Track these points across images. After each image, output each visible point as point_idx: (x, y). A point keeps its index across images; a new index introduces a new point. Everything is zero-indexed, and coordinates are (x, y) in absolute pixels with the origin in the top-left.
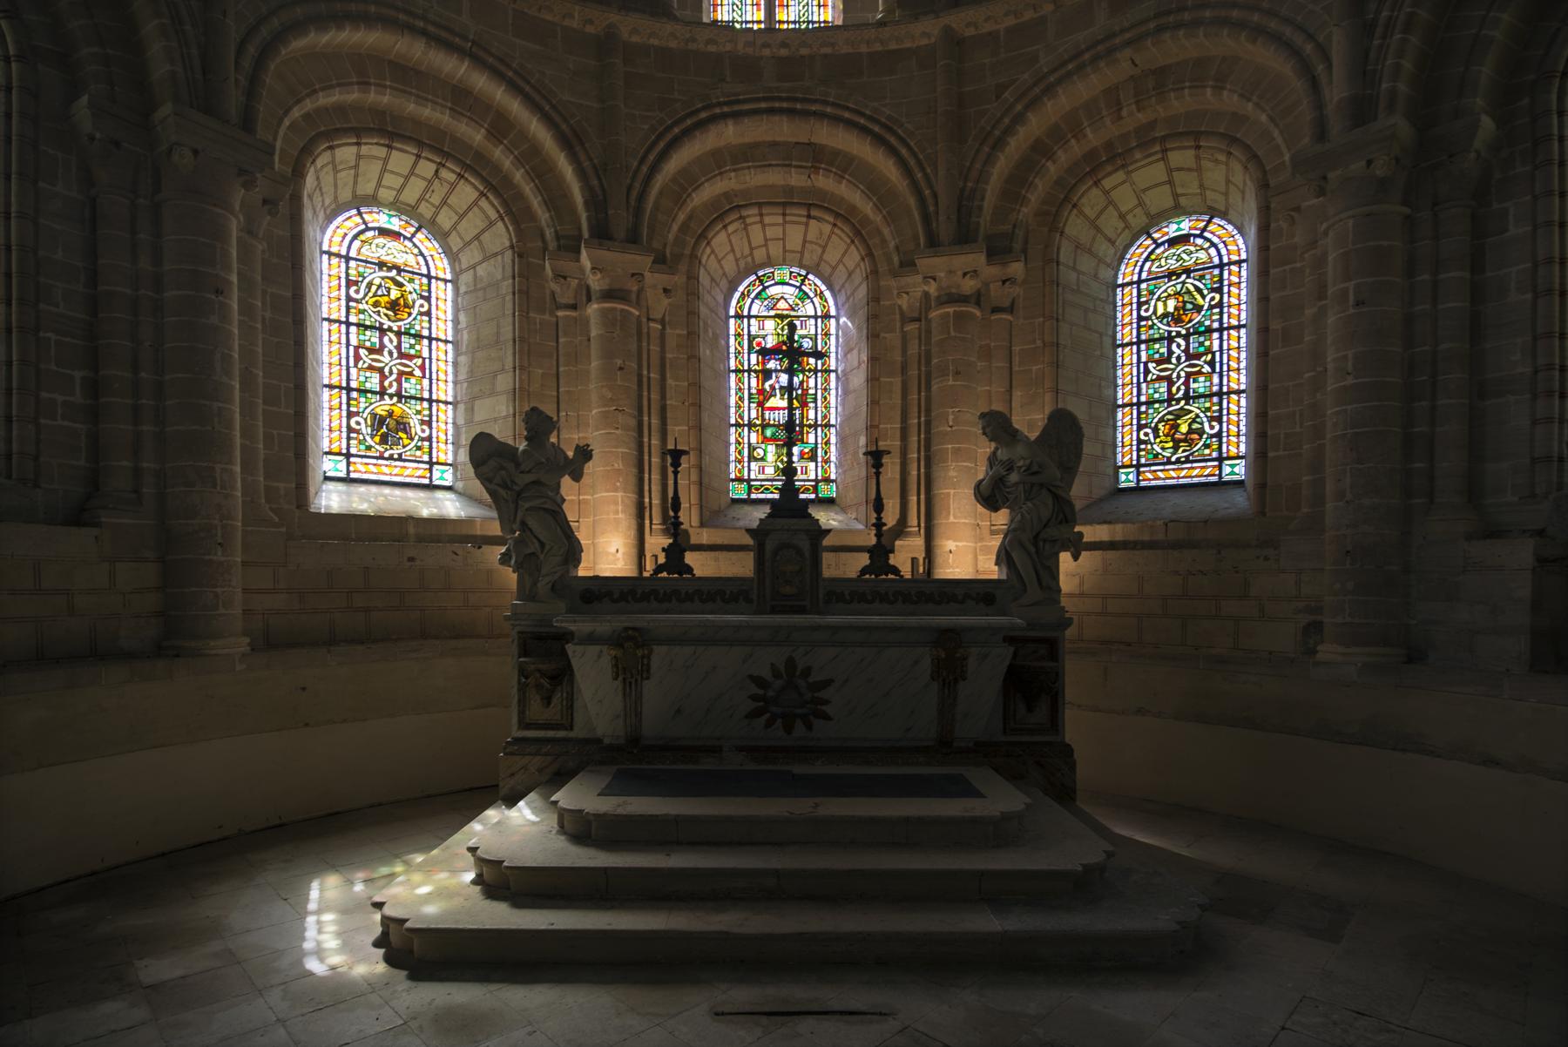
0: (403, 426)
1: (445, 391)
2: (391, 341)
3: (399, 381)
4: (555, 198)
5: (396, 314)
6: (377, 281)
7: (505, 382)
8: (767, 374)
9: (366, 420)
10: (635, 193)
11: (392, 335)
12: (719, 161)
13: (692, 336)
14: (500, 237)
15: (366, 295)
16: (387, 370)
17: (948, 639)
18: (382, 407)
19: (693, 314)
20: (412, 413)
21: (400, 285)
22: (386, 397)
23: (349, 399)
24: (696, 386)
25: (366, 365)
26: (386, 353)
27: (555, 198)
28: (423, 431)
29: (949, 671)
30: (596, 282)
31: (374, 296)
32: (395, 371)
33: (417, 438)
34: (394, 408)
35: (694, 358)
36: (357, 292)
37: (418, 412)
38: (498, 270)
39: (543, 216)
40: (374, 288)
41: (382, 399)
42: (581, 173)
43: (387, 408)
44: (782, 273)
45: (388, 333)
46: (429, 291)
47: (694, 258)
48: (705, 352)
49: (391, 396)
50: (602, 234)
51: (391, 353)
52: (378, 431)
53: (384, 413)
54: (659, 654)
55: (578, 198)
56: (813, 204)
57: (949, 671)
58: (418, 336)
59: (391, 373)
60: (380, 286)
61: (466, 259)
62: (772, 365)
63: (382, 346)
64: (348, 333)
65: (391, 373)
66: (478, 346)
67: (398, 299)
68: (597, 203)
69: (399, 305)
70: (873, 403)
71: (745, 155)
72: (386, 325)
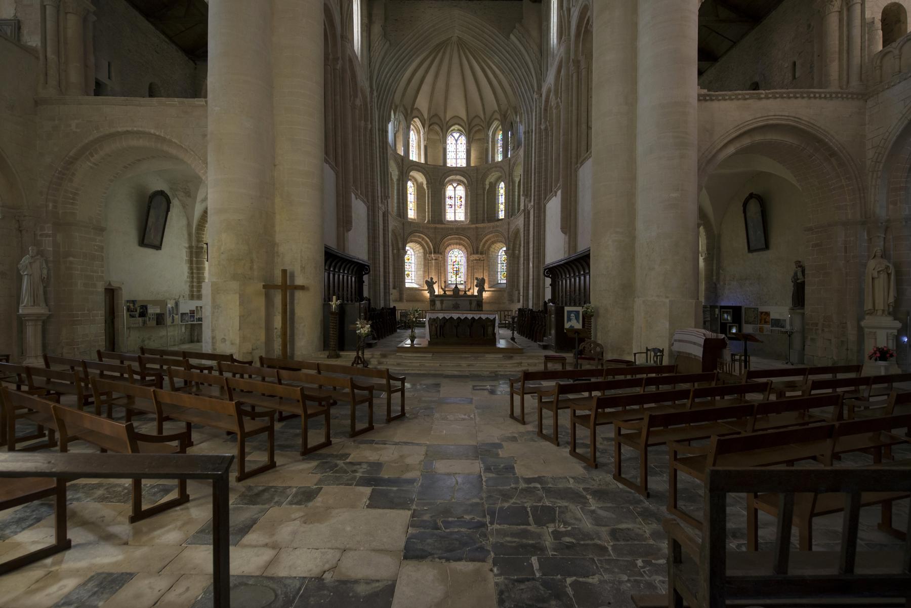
0: (409, 275)
4: (429, 247)
7: (422, 269)
8: (454, 265)
12: (448, 240)
13: (444, 262)
14: (422, 251)
17: (471, 300)
19: (444, 259)
20: (410, 273)
24: (445, 269)
27: (429, 247)
29: (471, 304)
30: (434, 258)
35: (444, 265)
38: (421, 255)
39: (427, 249)
42: (433, 245)
44: (456, 250)
47: (445, 252)
48: (446, 264)
50: (435, 253)
54: (444, 302)
55: (432, 247)
56: (460, 244)
57: (471, 304)
61: (416, 252)
62: (454, 264)
66: (418, 265)
68: (434, 248)
70: (467, 271)
71: (451, 239)
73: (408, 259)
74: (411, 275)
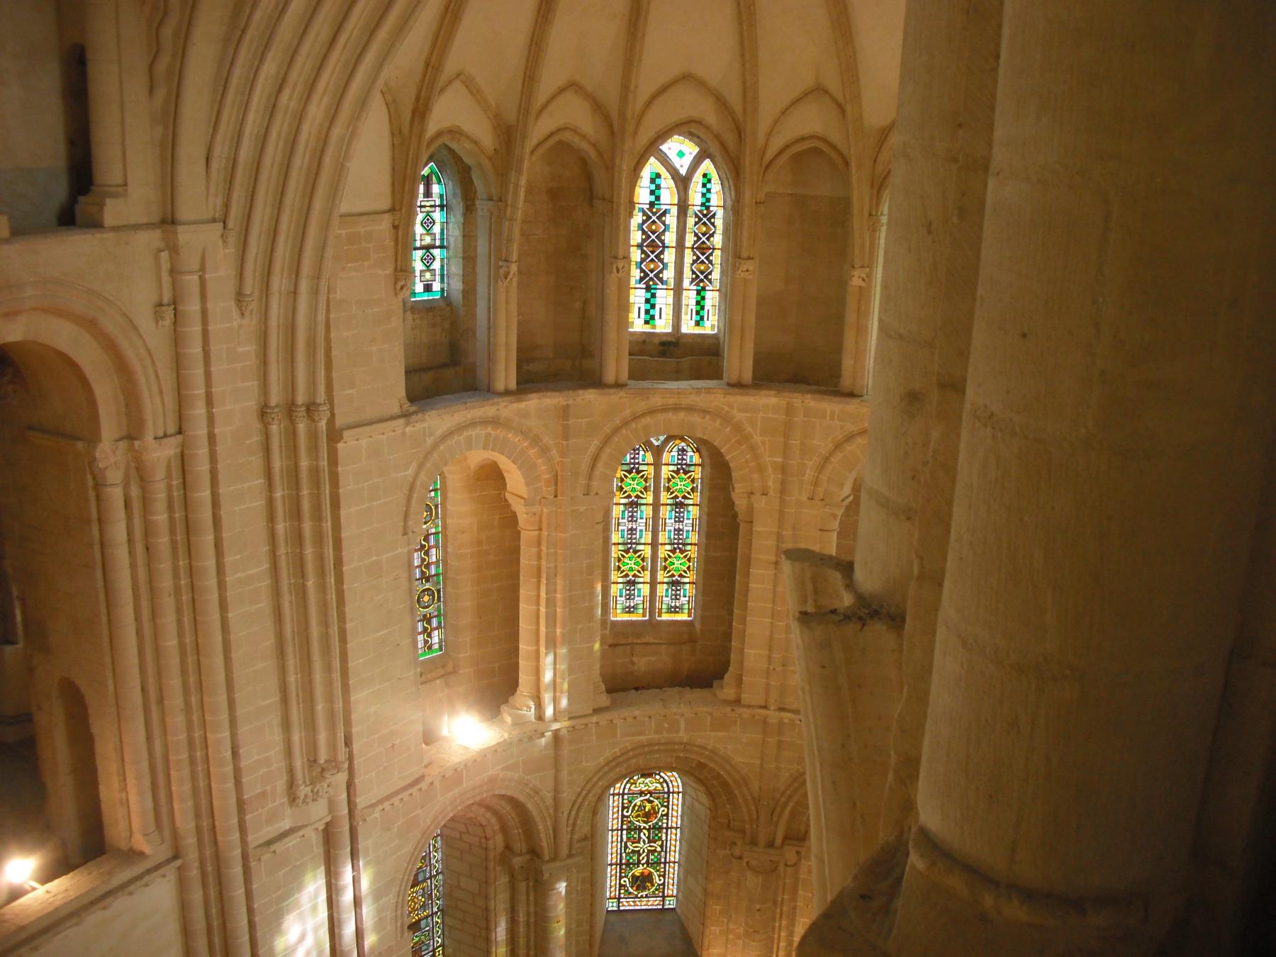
1: (674, 856)
2: (645, 834)
3: (648, 856)
5: (648, 819)
6: (638, 804)
9: (629, 879)
10: (776, 814)
11: (645, 831)
15: (632, 812)
16: (641, 851)
18: (638, 871)
21: (650, 801)
22: (641, 865)
23: (621, 869)
25: (630, 851)
26: (641, 842)
28: (660, 880)
31: (637, 811)
32: (646, 851)
33: (656, 885)
34: (645, 871)
36: (627, 812)
37: (658, 871)
40: (637, 808)
41: (638, 866)
43: (641, 871)
45: (644, 831)
46: (668, 802)
49: (643, 865)
51: (644, 842)
52: (636, 883)
53: (638, 874)
58: (661, 828)
59: (644, 851)
60: (640, 806)
63: (640, 838)
64: (622, 835)
65: (644, 851)
67: (649, 811)
69: (651, 814)
72: (643, 825)
73: (647, 816)
74: (657, 880)
